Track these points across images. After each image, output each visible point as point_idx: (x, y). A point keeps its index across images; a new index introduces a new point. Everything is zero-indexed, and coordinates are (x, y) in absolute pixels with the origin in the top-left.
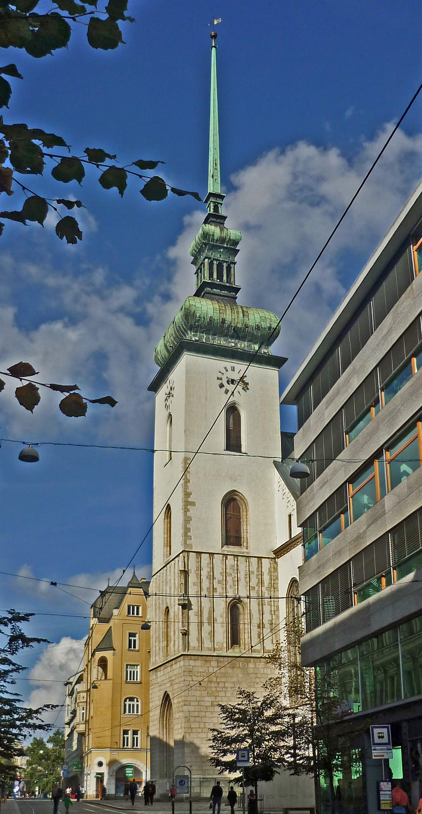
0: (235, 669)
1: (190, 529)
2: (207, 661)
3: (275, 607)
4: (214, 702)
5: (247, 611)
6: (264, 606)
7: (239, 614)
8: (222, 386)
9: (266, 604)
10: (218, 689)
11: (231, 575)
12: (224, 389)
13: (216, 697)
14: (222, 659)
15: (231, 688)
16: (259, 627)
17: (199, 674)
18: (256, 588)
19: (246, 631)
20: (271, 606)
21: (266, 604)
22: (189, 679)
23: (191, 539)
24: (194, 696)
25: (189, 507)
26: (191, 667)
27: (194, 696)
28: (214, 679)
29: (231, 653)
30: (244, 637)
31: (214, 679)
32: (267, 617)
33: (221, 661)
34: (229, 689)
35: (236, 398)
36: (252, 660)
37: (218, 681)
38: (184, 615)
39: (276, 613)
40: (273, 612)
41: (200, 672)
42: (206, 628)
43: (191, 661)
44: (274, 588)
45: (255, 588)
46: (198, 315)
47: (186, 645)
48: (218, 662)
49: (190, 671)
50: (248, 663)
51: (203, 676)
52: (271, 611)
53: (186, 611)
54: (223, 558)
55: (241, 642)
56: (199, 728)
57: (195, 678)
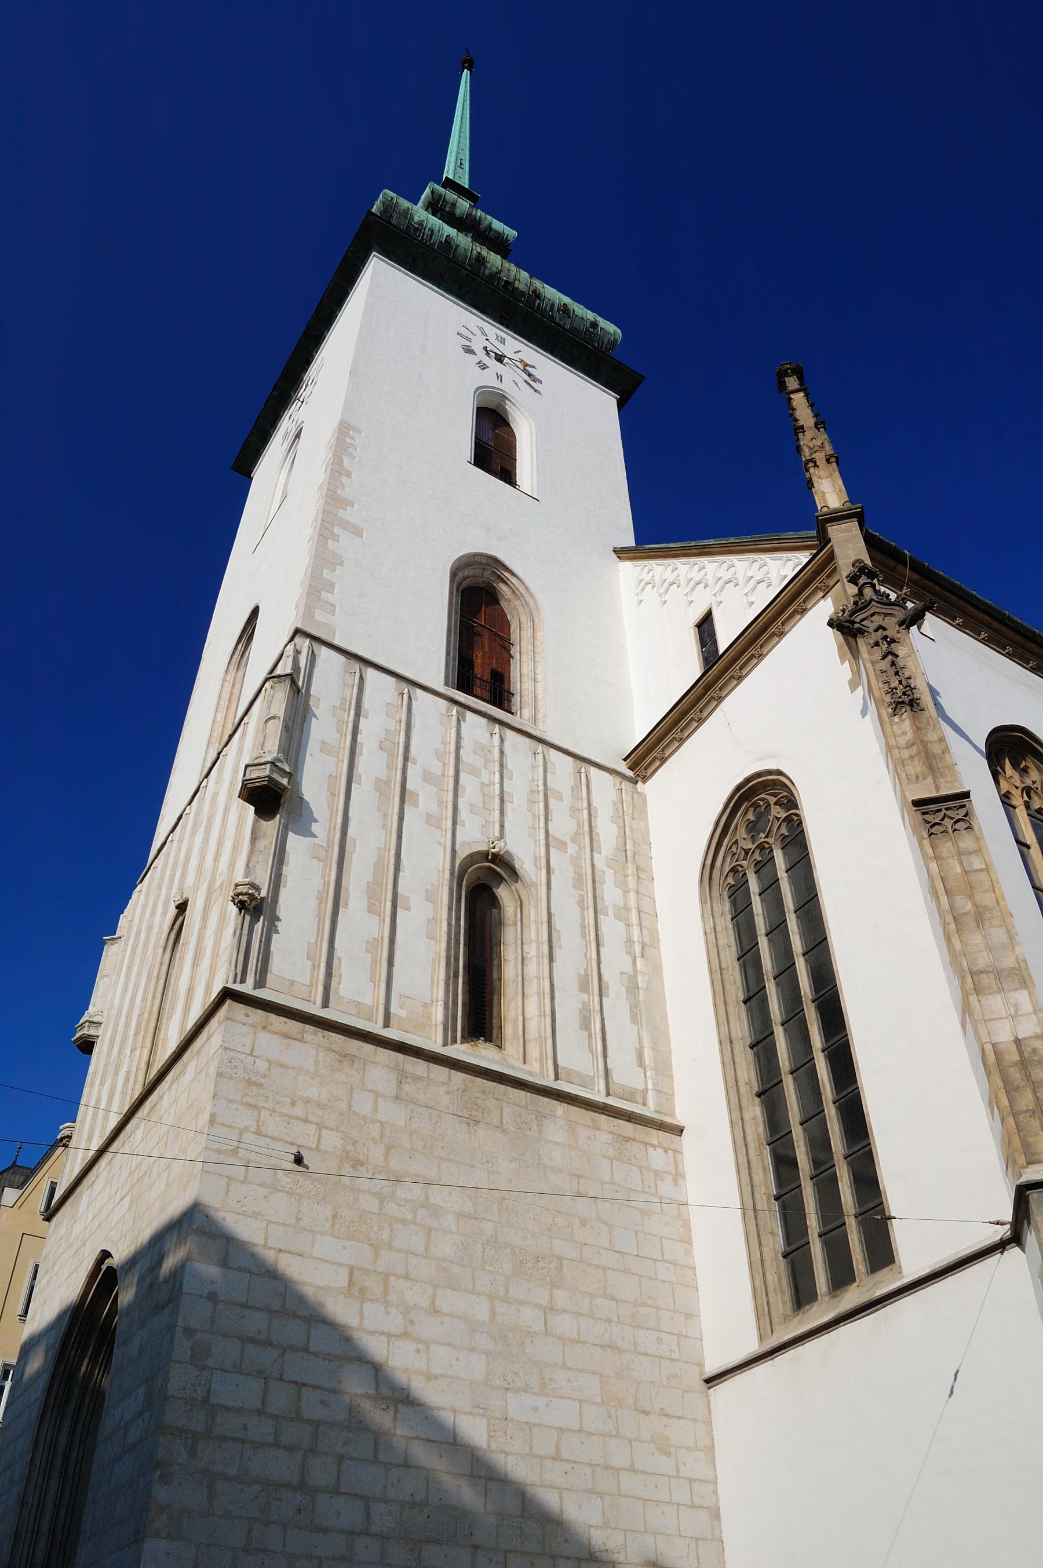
0: (482, 1132)
1: (332, 585)
2: (345, 1056)
3: (646, 933)
4: (364, 1270)
5: (535, 914)
6: (601, 918)
7: (500, 923)
8: (469, 351)
9: (611, 912)
10: (392, 1208)
11: (475, 772)
12: (473, 359)
13: (375, 1247)
14: (420, 1067)
15: (461, 1215)
16: (584, 987)
17: (299, 1110)
18: (572, 848)
19: (532, 989)
20: (628, 925)
21: (611, 912)
22: (244, 1119)
23: (333, 613)
24: (256, 1215)
25: (336, 530)
26: (262, 1066)
27: (256, 1215)
28: (377, 1153)
29: (461, 1051)
30: (519, 1005)
31: (377, 1153)
32: (616, 962)
33: (416, 1078)
34: (449, 1221)
35: (506, 387)
36: (560, 1108)
37: (394, 1164)
38: (261, 844)
39: (650, 951)
40: (638, 948)
41: (308, 1101)
42: (359, 924)
43: (264, 1038)
44: (638, 868)
45: (565, 844)
46: (416, 219)
47: (254, 957)
48: (403, 1076)
49: (249, 1082)
50: (540, 1116)
51: (320, 1126)
52: (630, 941)
53: (271, 827)
54: (448, 710)
55: (508, 1030)
56: (261, 1412)
57: (273, 1125)
